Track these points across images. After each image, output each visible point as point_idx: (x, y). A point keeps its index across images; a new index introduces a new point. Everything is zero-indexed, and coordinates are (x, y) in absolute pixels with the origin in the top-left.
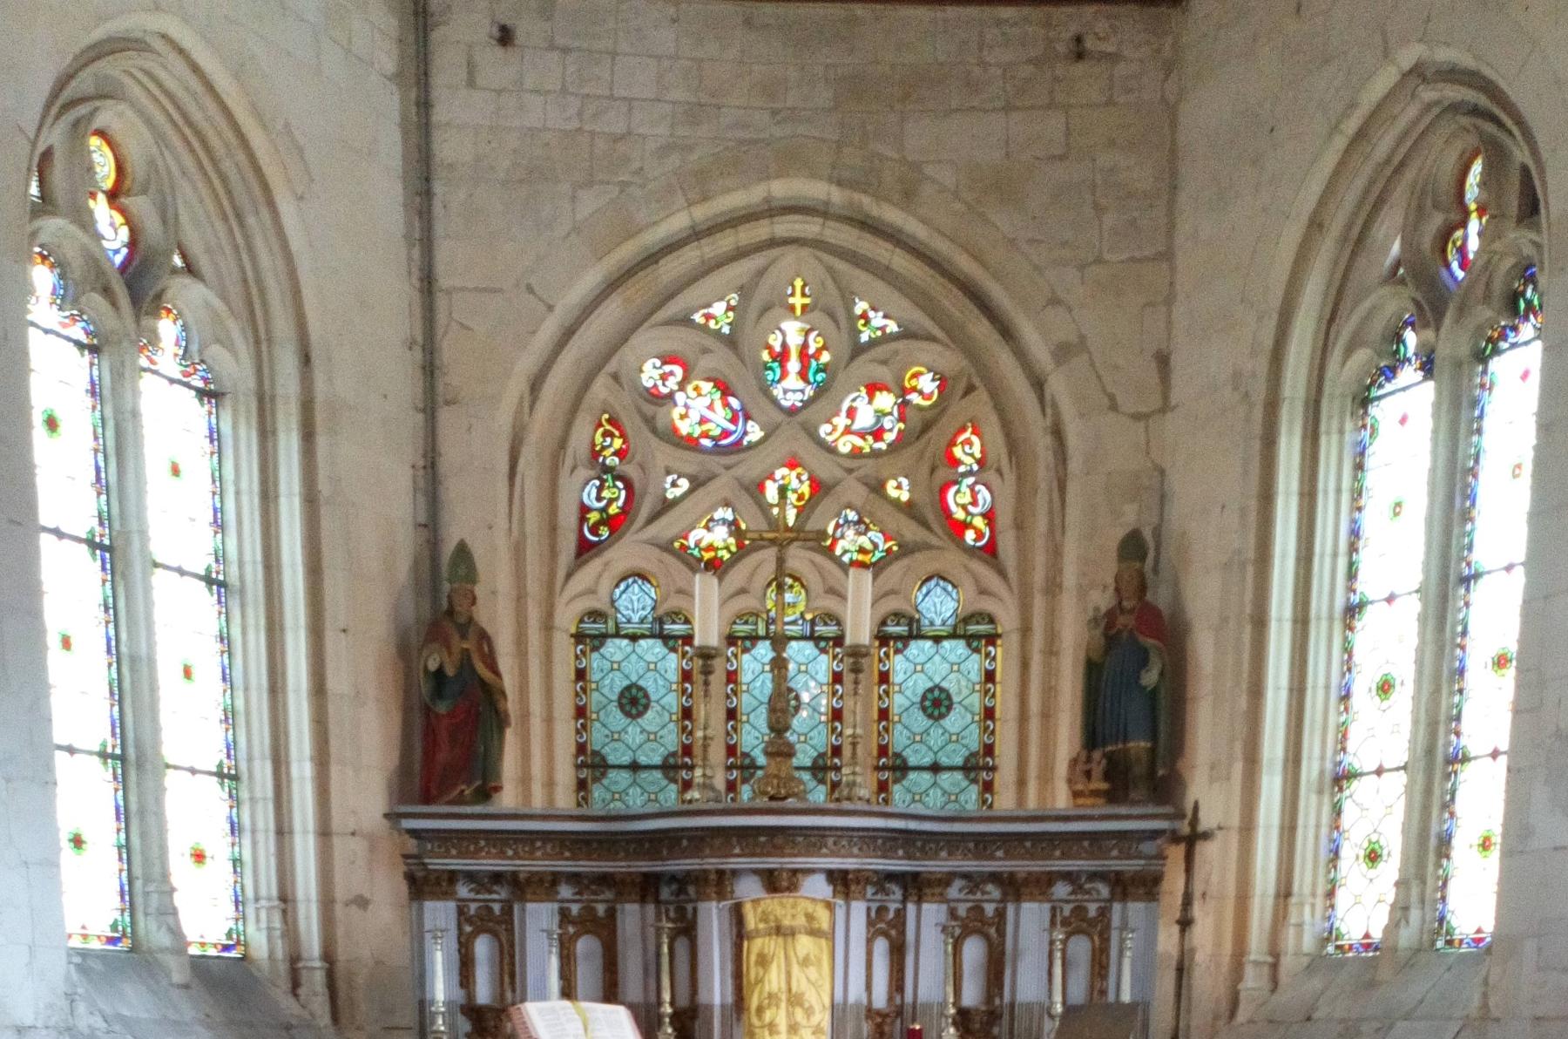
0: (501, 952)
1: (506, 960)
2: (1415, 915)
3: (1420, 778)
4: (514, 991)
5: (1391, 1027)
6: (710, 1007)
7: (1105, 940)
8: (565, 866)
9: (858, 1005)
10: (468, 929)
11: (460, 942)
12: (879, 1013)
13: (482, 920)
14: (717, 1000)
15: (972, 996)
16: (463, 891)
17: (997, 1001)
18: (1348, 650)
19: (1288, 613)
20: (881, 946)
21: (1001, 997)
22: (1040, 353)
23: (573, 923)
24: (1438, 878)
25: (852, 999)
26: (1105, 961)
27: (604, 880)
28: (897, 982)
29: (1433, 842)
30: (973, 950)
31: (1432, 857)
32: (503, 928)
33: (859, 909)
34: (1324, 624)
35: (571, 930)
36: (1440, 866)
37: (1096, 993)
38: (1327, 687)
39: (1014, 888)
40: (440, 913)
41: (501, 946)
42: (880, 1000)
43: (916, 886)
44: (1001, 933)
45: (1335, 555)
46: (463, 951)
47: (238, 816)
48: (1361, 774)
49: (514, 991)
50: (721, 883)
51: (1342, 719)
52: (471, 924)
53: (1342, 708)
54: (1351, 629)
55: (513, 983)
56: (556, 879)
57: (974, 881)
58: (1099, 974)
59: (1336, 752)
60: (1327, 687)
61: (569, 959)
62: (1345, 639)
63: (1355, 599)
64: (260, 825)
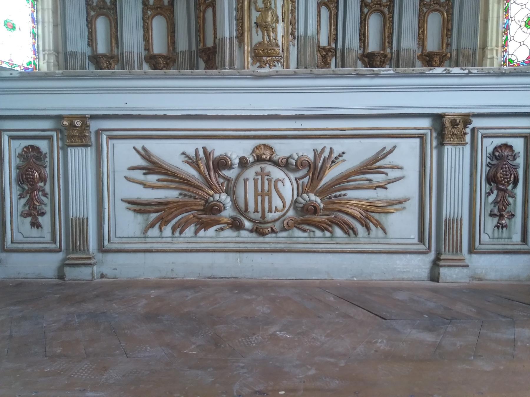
0: (111, 26)
1: (114, 30)
4: (118, 48)
6: (223, 40)
7: (451, 13)
9: (313, 38)
10: (92, 13)
11: (87, 20)
12: (324, 48)
13: (100, 8)
14: (227, 35)
15: (373, 46)
17: (388, 50)
20: (324, 12)
21: (391, 49)
23: (151, 9)
25: (309, 33)
26: (450, 28)
35: (149, 13)
37: (445, 45)
41: (110, 20)
42: (324, 42)
44: (392, 12)
46: (90, 26)
47: (37, 16)
49: (118, 48)
55: (117, 43)
58: (447, 35)
61: (148, 29)
64: (46, 20)
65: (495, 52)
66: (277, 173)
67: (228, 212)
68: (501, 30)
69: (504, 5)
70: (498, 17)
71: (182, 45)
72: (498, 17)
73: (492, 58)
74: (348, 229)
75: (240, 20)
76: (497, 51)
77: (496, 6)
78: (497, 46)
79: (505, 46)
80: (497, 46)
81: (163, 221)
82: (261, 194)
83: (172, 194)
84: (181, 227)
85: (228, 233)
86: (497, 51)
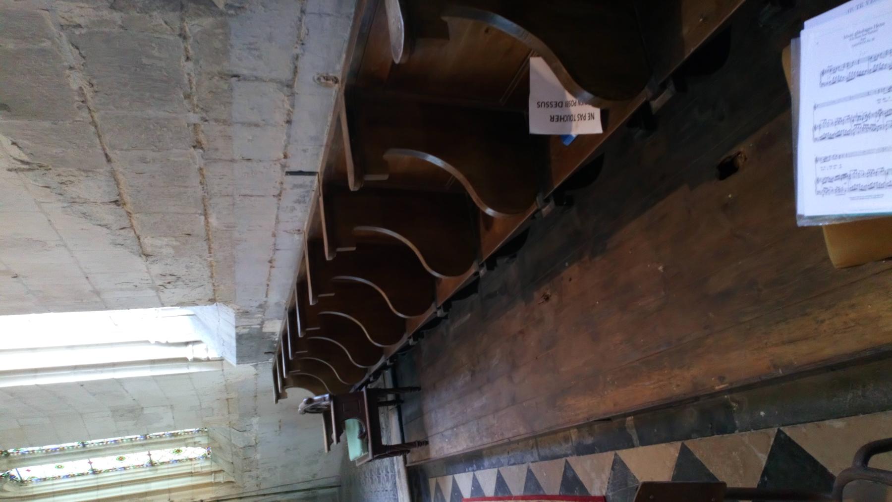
2: (197, 440)
3: (151, 447)
5: (234, 445)
18: (108, 471)
19: (95, 493)
24: (184, 434)
29: (173, 438)
31: (178, 438)
34: (99, 480)
36: (181, 434)
38: (121, 475)
45: (75, 481)
48: (151, 459)
51: (132, 468)
53: (128, 468)
54: (101, 471)
59: (143, 467)
60: (121, 475)
62: (105, 472)
63: (91, 472)
65: (196, 466)
68: (178, 464)
69: (158, 465)
70: (168, 468)
72: (168, 468)
73: (202, 468)
76: (195, 464)
77: (159, 472)
78: (191, 465)
79: (191, 460)
80: (191, 465)
86: (195, 464)
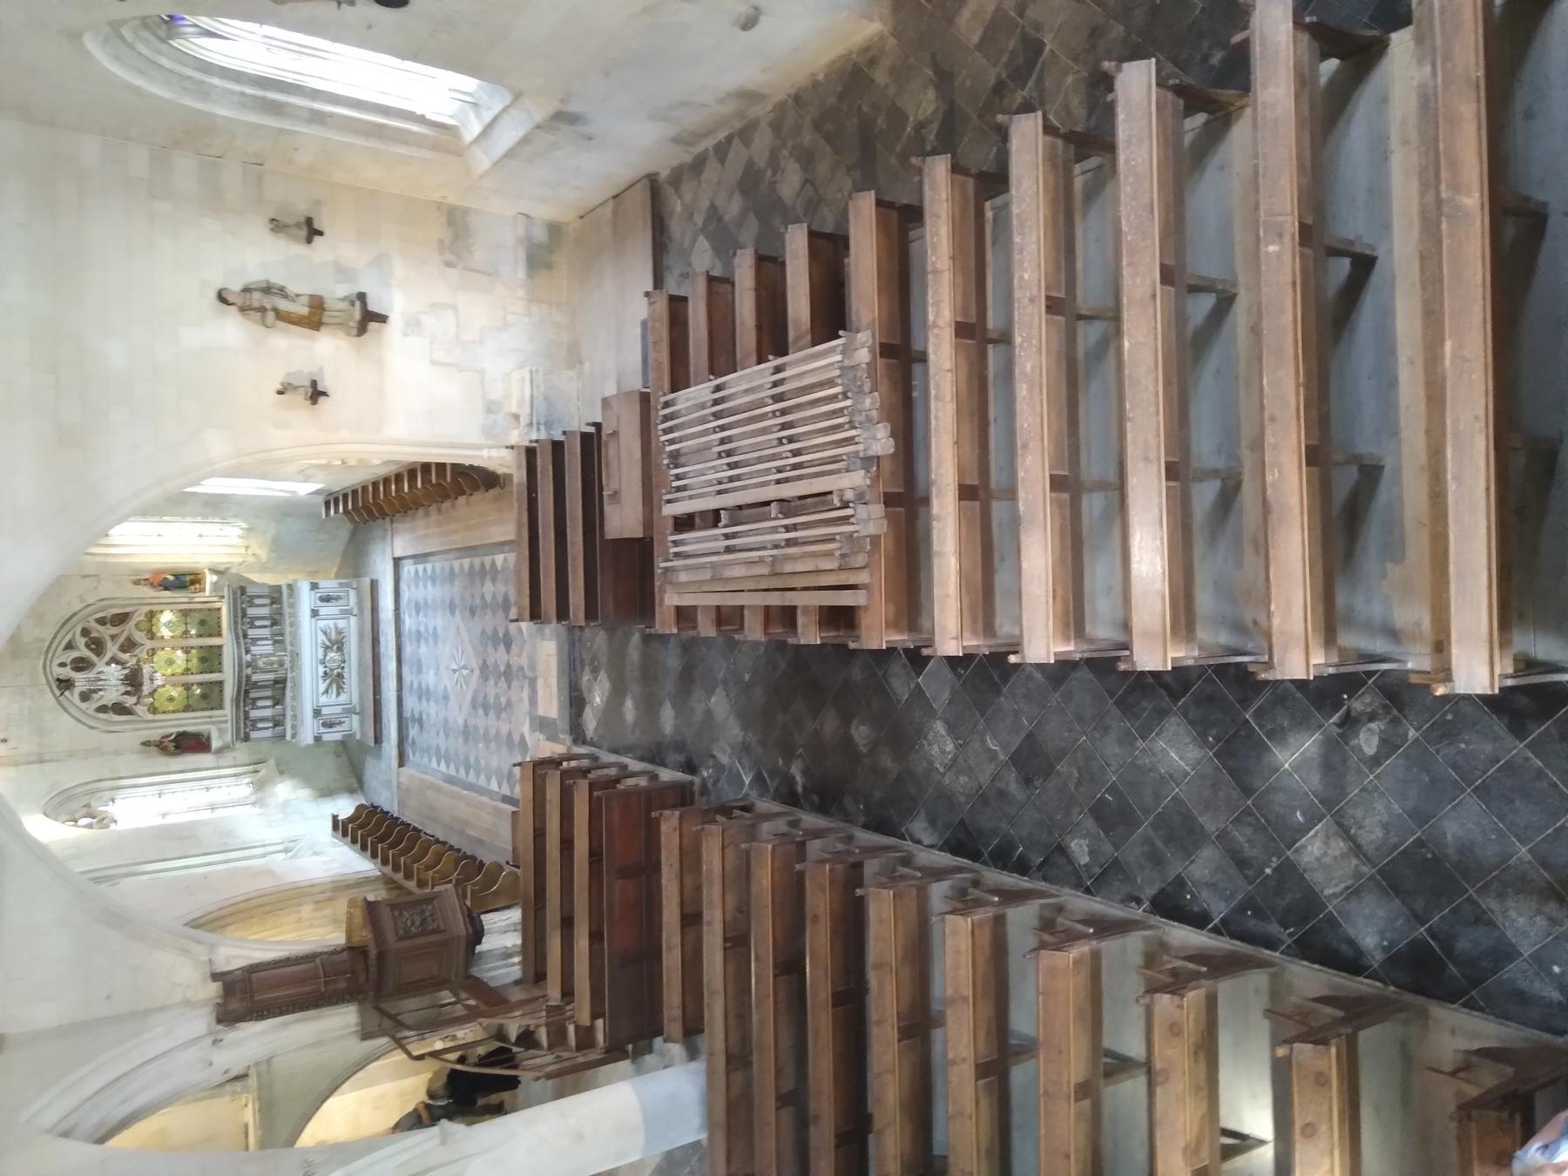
8: (242, 709)
16: (247, 730)
20: (259, 643)
22: (81, 606)
27: (244, 702)
28: (266, 639)
30: (258, 623)
32: (255, 721)
33: (252, 648)
39: (244, 615)
40: (253, 735)
42: (270, 642)
43: (245, 636)
50: (248, 677)
52: (255, 728)
56: (245, 711)
57: (243, 624)
66: (328, 658)
67: (339, 670)
71: (268, 693)
74: (343, 638)
75: (268, 672)
81: (342, 688)
82: (334, 661)
83: (334, 686)
84: (344, 683)
85: (346, 670)
